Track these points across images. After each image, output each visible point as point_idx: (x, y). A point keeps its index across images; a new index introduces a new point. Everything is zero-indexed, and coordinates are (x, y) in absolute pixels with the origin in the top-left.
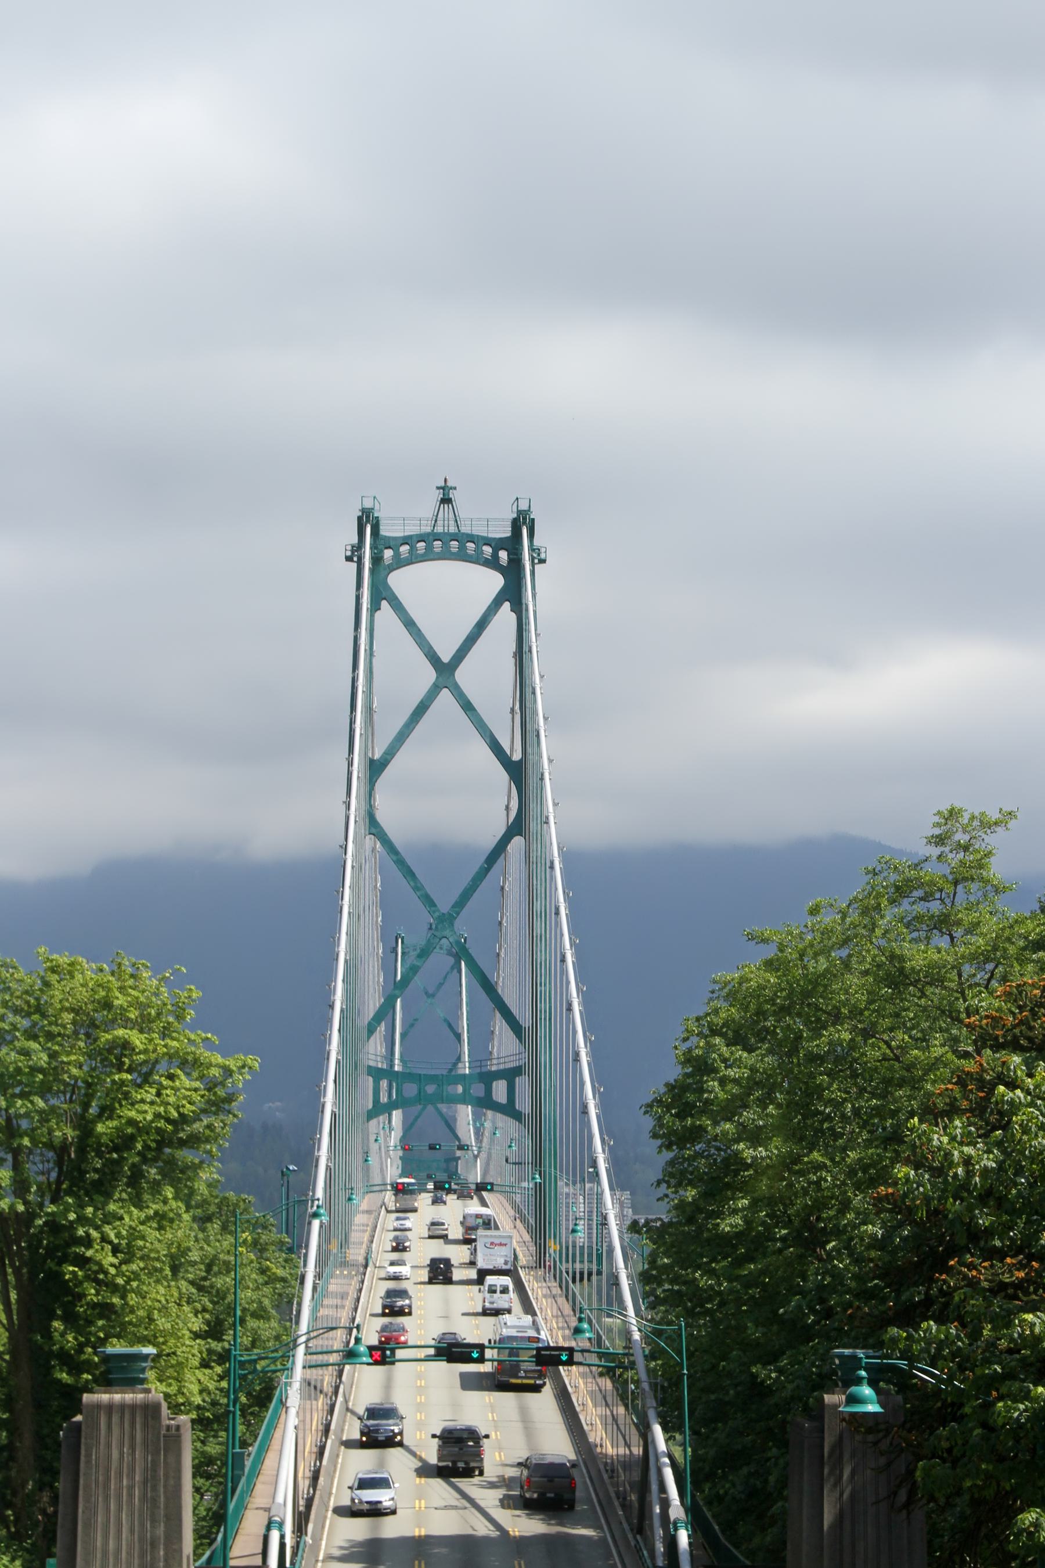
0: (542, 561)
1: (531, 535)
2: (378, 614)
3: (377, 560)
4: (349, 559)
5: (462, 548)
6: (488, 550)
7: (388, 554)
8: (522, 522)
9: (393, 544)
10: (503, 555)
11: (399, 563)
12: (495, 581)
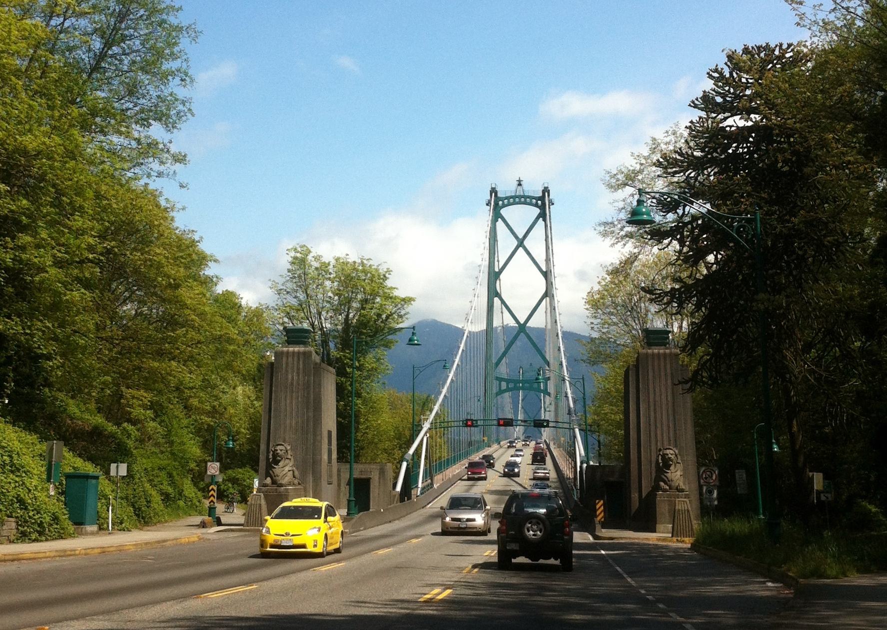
0: (553, 204)
2: (497, 223)
3: (496, 204)
4: (487, 205)
5: (525, 200)
6: (534, 201)
7: (500, 203)
8: (546, 190)
9: (502, 199)
10: (539, 202)
11: (504, 206)
12: (537, 211)
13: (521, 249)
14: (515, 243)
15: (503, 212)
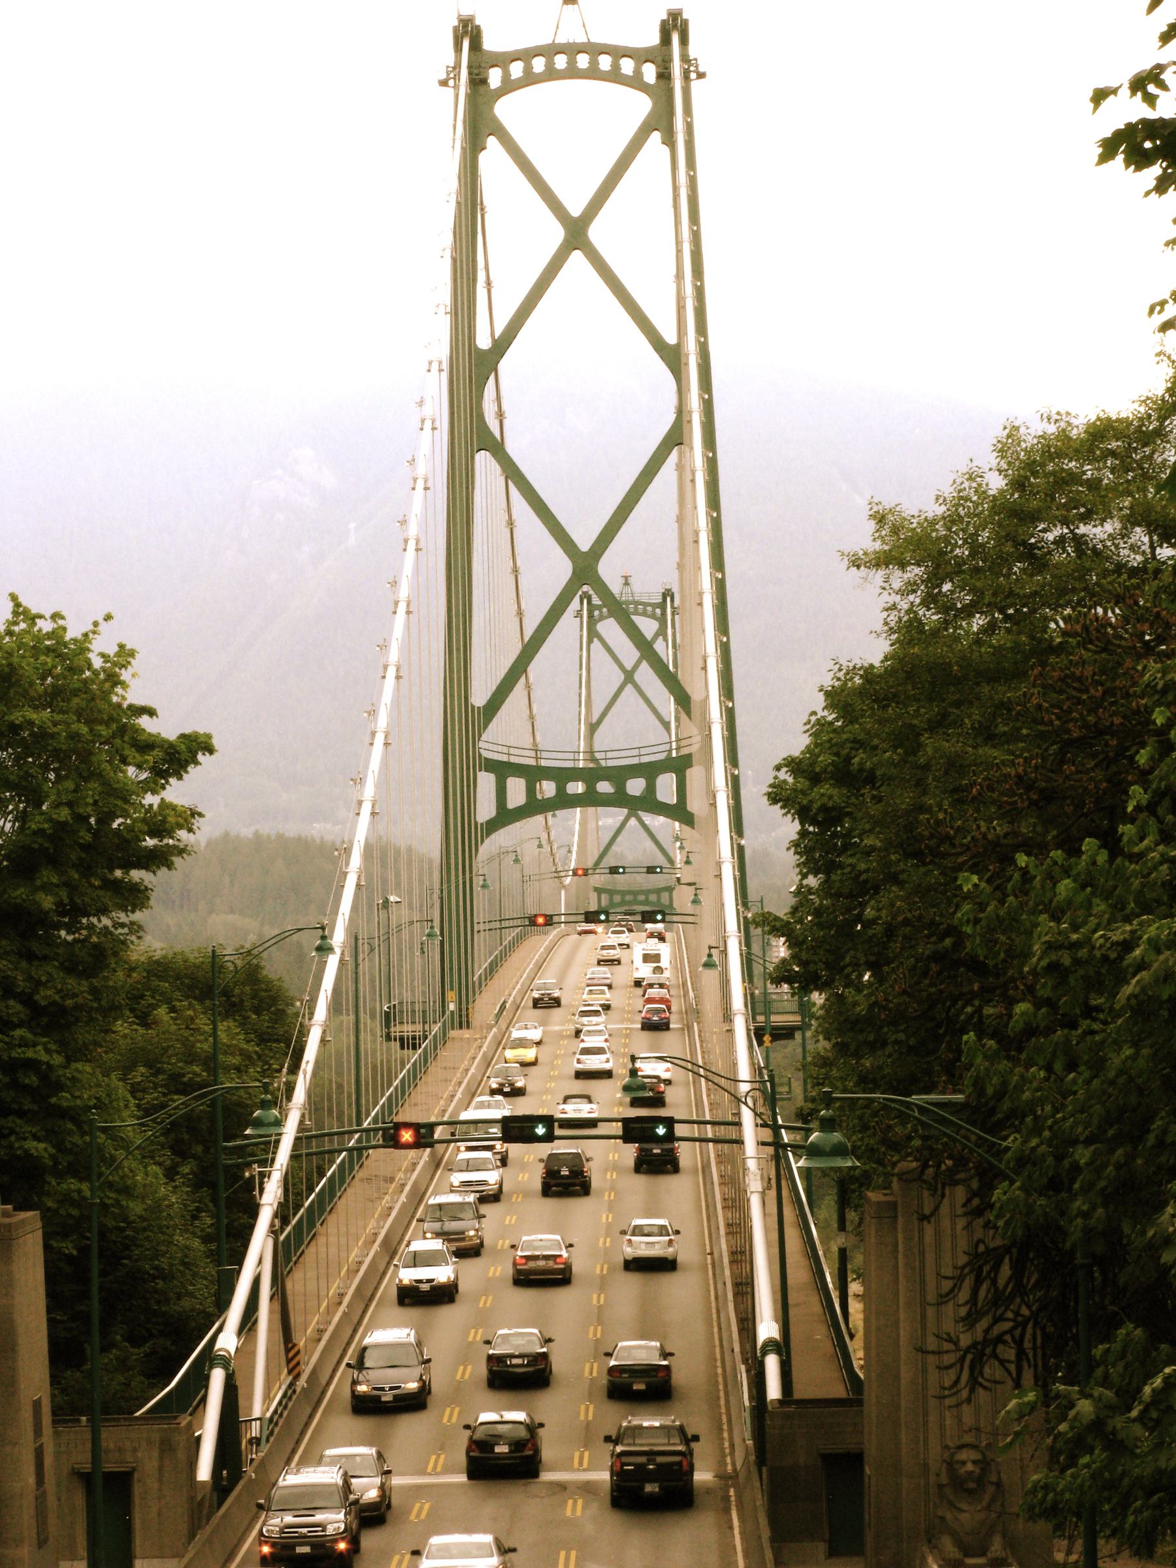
0: (701, 76)
1: (684, 41)
2: (483, 157)
3: (478, 81)
4: (444, 83)
5: (594, 63)
6: (627, 66)
9: (503, 60)
10: (650, 73)
11: (508, 86)
13: (577, 257)
14: (557, 234)
15: (505, 110)
